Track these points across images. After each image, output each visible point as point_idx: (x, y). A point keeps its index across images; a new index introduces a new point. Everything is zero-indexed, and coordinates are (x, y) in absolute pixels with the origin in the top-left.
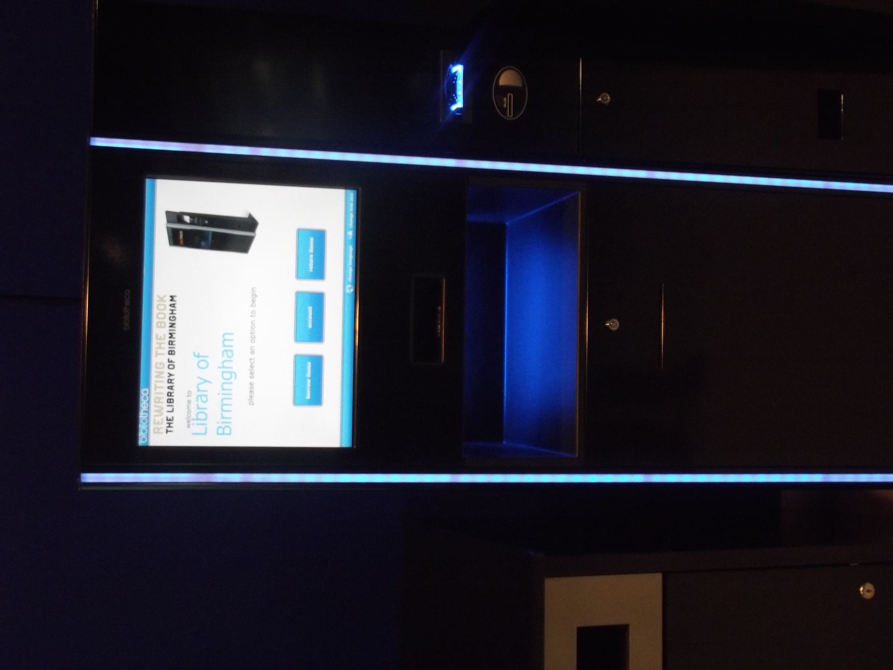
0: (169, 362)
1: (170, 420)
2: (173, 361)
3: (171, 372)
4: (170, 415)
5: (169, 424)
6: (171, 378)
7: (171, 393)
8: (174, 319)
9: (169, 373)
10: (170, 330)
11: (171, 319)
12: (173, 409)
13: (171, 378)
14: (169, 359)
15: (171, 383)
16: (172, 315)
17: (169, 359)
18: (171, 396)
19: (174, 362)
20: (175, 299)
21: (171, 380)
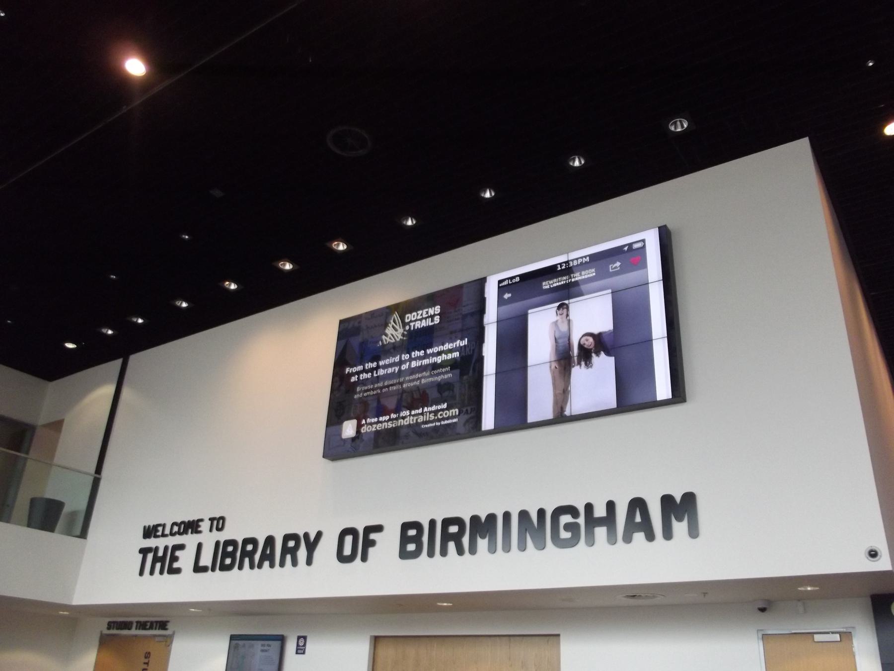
0: (369, 530)
1: (174, 559)
2: (371, 550)
3: (327, 549)
4: (186, 560)
5: (162, 560)
6: (302, 553)
7: (251, 555)
8: (565, 535)
9: (319, 535)
10: (507, 516)
11: (566, 519)
12: (204, 569)
13: (302, 553)
14: (378, 529)
15: (285, 550)
16: (581, 520)
17: (378, 529)
18: (244, 554)
19: (364, 559)
20: (680, 528)
21: (293, 552)
